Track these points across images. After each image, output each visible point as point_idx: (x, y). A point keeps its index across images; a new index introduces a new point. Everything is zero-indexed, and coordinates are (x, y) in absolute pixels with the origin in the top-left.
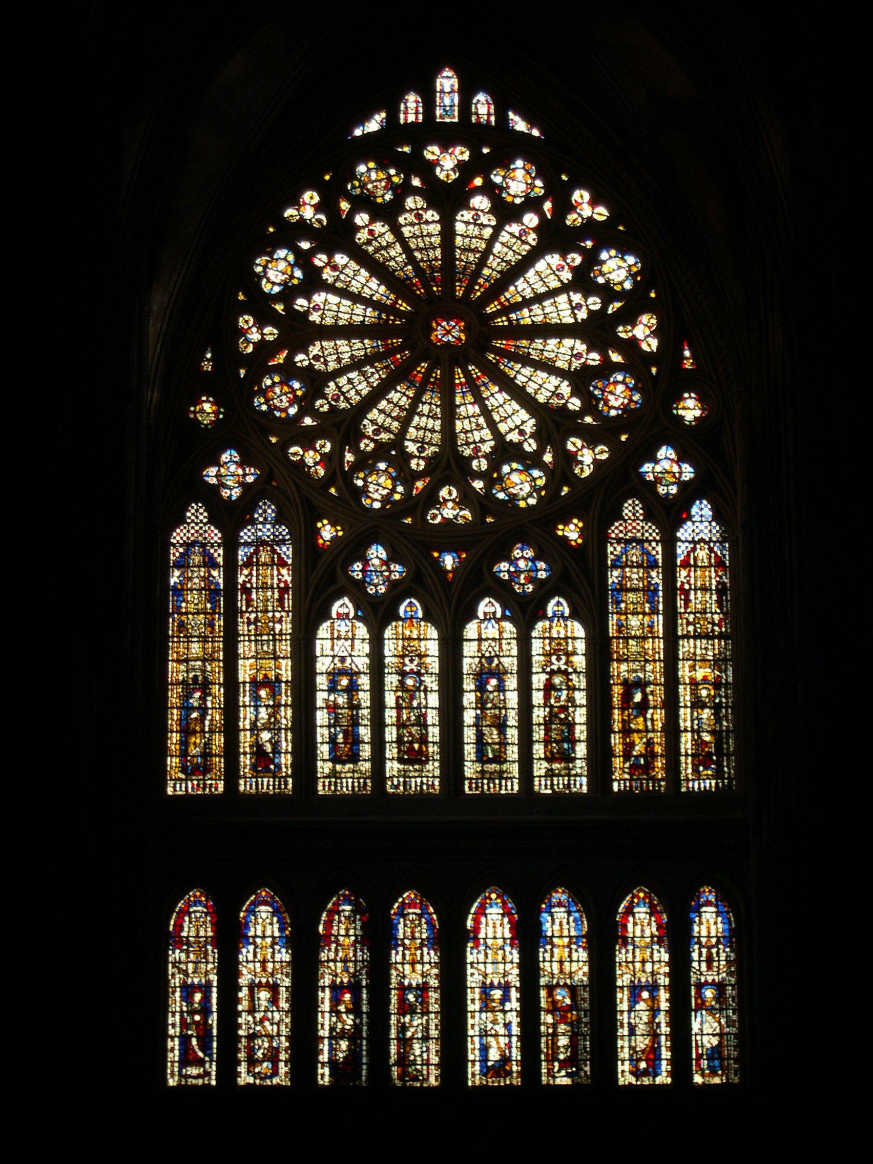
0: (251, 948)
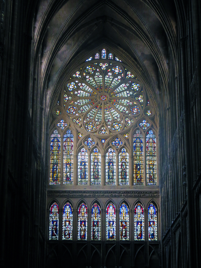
0: (65, 214)
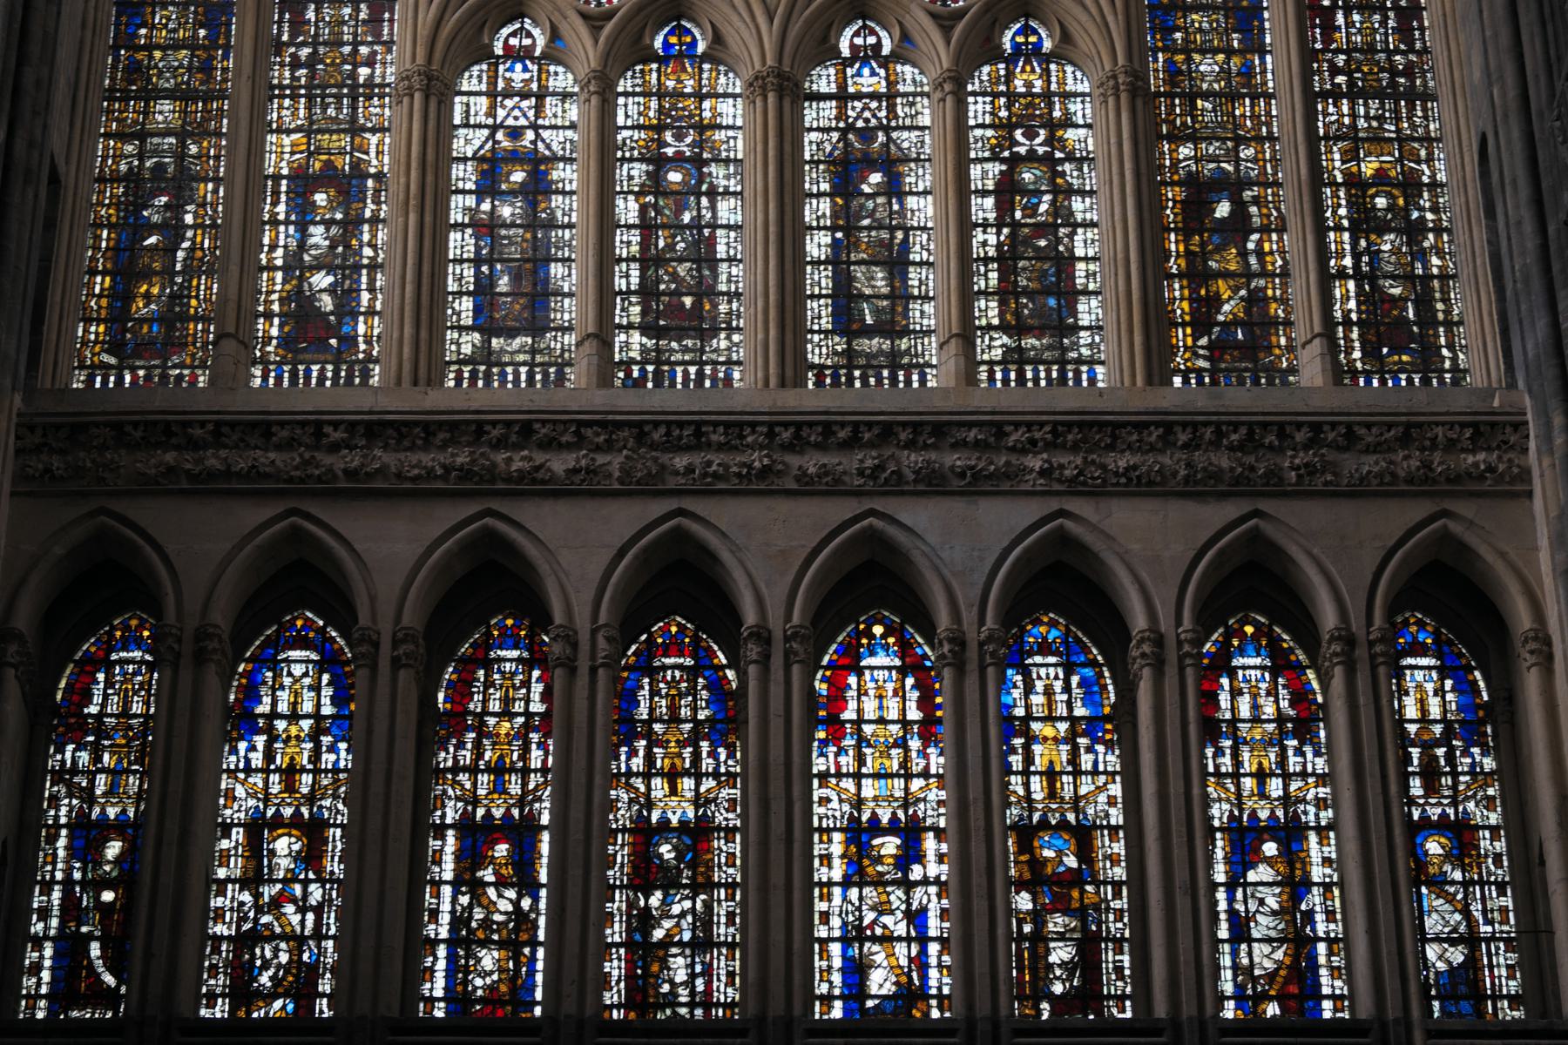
0: (260, 741)
